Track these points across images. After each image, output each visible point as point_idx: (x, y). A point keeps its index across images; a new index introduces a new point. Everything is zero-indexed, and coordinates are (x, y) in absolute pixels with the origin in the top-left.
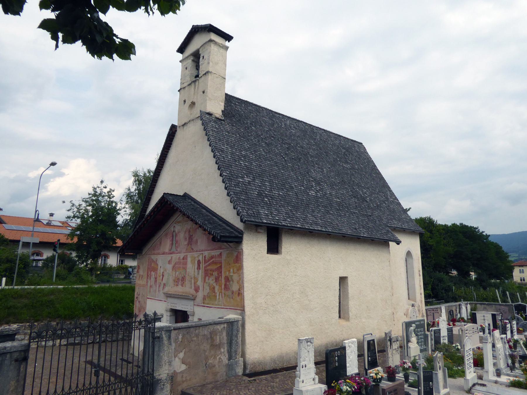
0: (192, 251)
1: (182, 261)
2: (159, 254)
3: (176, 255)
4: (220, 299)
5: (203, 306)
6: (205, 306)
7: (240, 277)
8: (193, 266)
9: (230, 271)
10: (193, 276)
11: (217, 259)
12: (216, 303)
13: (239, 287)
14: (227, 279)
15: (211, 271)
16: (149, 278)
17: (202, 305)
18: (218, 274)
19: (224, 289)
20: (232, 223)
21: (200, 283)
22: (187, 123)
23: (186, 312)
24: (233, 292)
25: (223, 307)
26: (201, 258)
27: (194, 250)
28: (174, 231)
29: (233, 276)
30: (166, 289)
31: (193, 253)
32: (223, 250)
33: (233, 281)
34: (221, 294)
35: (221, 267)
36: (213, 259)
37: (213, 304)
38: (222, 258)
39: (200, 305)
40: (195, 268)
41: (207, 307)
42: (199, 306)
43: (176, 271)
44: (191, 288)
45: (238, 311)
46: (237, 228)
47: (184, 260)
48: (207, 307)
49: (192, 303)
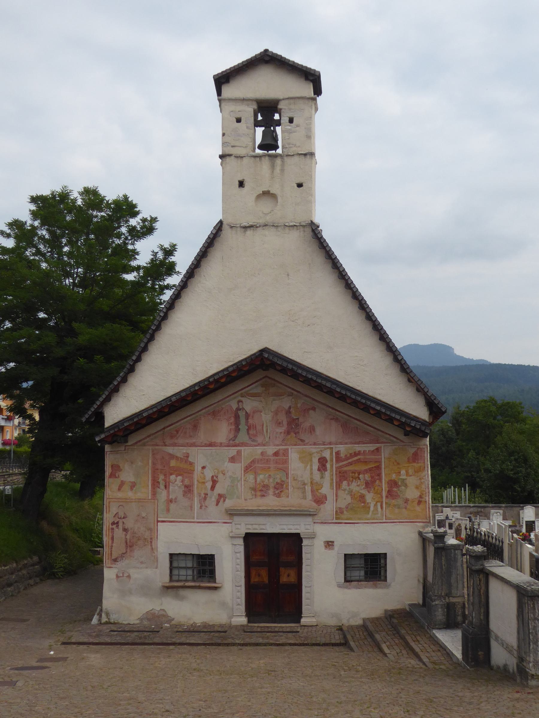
0: (301, 443)
1: (272, 458)
2: (193, 445)
3: (252, 448)
4: (377, 510)
5: (336, 523)
6: (341, 523)
7: (422, 481)
8: (306, 467)
9: (400, 473)
10: (307, 479)
11: (368, 457)
12: (369, 516)
13: (419, 494)
14: (393, 484)
15: (353, 473)
16: (162, 486)
17: (335, 521)
18: (372, 477)
19: (387, 497)
20: (401, 409)
21: (326, 489)
22: (257, 227)
23: (298, 535)
24: (407, 501)
25: (384, 521)
26: (327, 454)
27: (306, 442)
28: (238, 409)
29: (406, 479)
30: (229, 503)
31: (305, 447)
32: (382, 445)
33: (406, 486)
34: (379, 504)
35: (379, 468)
36: (359, 457)
37: (360, 519)
38: (381, 455)
39: (330, 521)
40: (311, 469)
41: (345, 523)
42: (325, 523)
43: (256, 474)
44: (305, 498)
45: (418, 524)
46: (415, 416)
47: (276, 456)
48: (345, 523)
49: (310, 519)
